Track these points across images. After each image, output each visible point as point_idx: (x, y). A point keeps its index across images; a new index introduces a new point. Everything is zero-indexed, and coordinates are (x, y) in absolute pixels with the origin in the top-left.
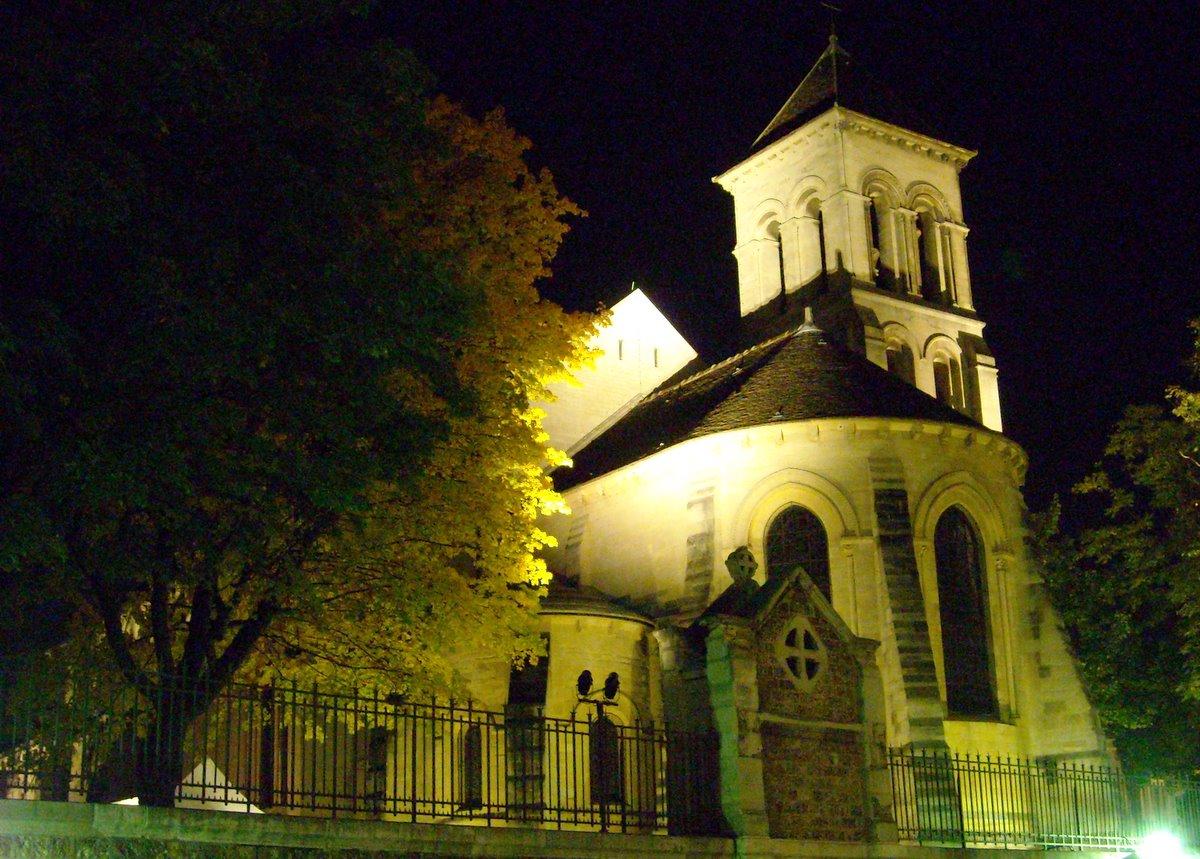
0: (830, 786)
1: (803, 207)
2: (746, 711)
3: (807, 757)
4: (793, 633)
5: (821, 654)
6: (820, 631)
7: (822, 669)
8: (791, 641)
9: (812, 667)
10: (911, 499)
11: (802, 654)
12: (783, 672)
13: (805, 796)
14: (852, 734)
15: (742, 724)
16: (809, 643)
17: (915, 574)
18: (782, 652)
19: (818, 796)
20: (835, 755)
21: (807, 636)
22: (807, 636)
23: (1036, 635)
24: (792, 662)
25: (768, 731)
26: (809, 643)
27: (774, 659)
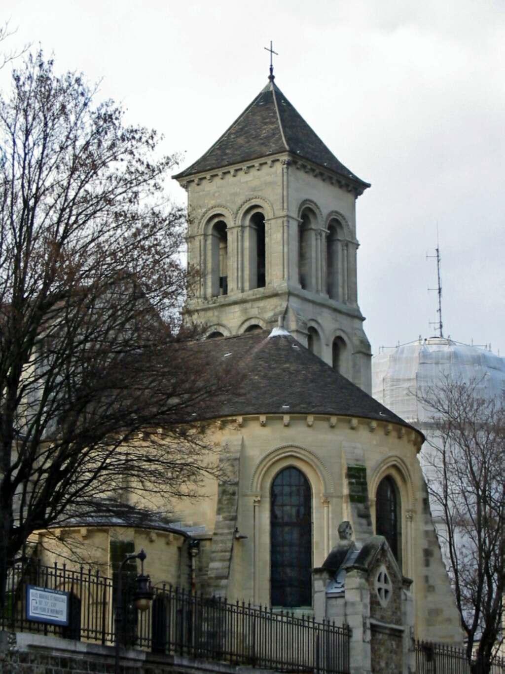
0: (392, 658)
1: (249, 217)
2: (366, 617)
3: (383, 644)
4: (380, 574)
5: (390, 587)
6: (390, 573)
7: (390, 594)
8: (379, 580)
9: (386, 591)
10: (368, 472)
11: (383, 586)
12: (376, 596)
13: (383, 664)
14: (401, 631)
15: (364, 624)
16: (386, 581)
17: (369, 524)
18: (377, 585)
19: (387, 664)
20: (394, 643)
21: (385, 576)
22: (385, 576)
23: (427, 564)
24: (380, 590)
25: (374, 629)
26: (386, 581)
27: (373, 589)
